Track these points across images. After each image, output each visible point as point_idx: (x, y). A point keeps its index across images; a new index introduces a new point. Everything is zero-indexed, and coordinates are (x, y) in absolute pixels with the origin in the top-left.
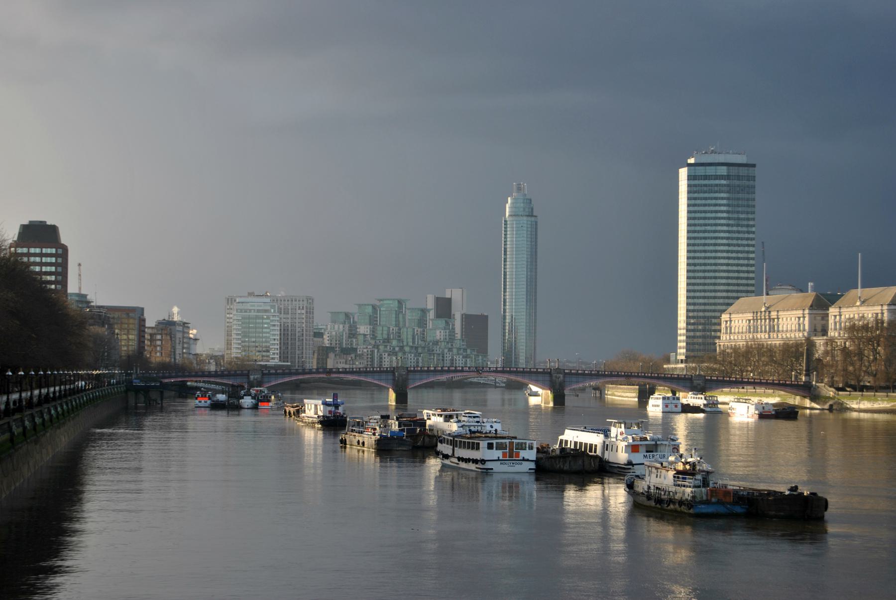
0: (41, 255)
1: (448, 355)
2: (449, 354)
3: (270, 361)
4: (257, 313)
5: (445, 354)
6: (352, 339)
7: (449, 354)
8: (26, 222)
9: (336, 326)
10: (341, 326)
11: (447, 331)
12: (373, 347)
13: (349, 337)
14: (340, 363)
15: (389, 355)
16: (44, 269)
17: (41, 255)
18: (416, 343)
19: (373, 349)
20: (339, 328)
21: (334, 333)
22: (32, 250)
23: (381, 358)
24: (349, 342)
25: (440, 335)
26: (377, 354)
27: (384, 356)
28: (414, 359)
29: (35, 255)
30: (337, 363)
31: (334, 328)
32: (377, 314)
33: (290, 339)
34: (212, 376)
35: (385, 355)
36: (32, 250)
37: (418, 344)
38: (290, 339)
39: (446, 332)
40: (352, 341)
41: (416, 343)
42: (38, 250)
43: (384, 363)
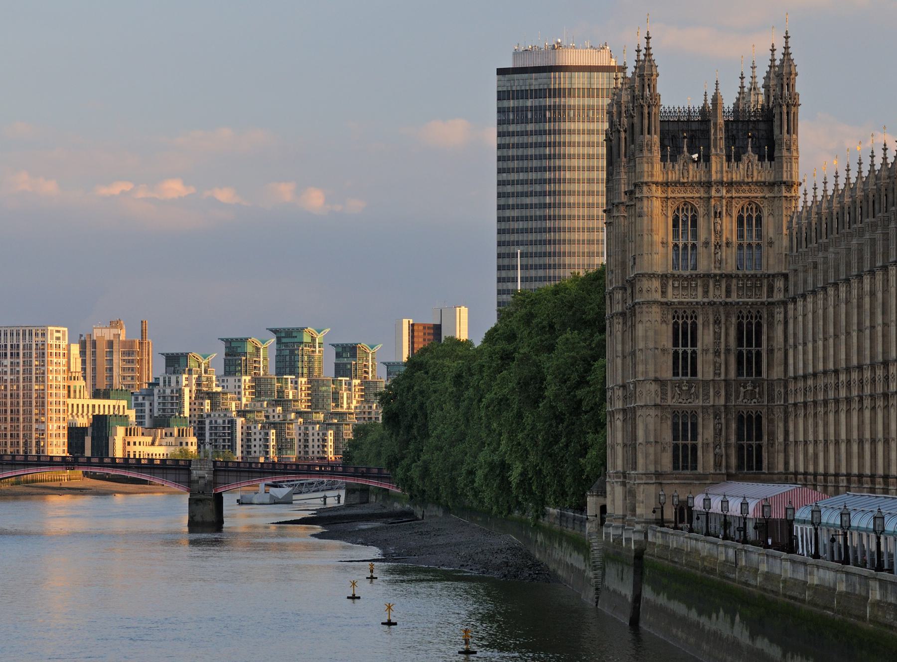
9: (173, 378)
14: (135, 443)
18: (345, 406)
21: (168, 391)
23: (249, 434)
24: (195, 407)
30: (129, 444)
31: (170, 382)
37: (349, 408)
41: (345, 406)
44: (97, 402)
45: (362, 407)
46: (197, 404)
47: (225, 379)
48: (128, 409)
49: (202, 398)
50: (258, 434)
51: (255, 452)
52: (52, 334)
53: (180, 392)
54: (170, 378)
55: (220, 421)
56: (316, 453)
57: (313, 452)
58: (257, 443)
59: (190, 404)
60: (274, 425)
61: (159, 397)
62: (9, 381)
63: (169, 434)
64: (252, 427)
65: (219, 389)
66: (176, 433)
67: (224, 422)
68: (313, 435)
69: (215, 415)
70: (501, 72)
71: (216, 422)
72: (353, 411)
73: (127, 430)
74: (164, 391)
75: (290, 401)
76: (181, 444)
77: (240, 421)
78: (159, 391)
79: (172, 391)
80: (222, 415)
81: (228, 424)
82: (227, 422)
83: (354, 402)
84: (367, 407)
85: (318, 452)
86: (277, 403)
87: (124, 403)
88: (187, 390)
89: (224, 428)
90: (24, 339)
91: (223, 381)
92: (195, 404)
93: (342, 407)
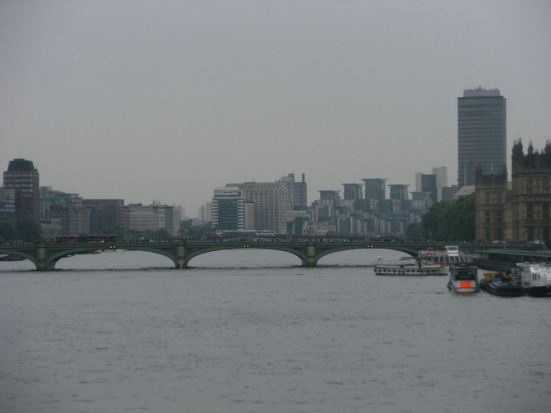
0: (21, 178)
4: (228, 197)
6: (335, 210)
8: (12, 160)
9: (324, 201)
11: (424, 201)
12: (350, 216)
13: (334, 209)
15: (362, 221)
16: (22, 185)
17: (21, 178)
18: (395, 211)
19: (350, 217)
20: (326, 202)
21: (322, 206)
22: (16, 175)
23: (356, 224)
24: (333, 213)
25: (418, 205)
26: (353, 221)
27: (358, 222)
28: (384, 224)
29: (18, 178)
31: (322, 203)
33: (269, 213)
35: (358, 221)
36: (16, 175)
37: (397, 211)
38: (269, 213)
39: (423, 202)
40: (335, 212)
41: (395, 211)
42: (19, 175)
43: (358, 230)
44: (296, 212)
51: (358, 231)
52: (281, 185)
53: (327, 207)
59: (331, 211)
60: (366, 220)
61: (318, 209)
63: (324, 224)
64: (357, 221)
65: (343, 206)
66: (327, 224)
67: (345, 219)
68: (382, 224)
70: (459, 99)
72: (398, 213)
73: (309, 223)
74: (320, 206)
75: (372, 210)
76: (330, 228)
77: (352, 219)
79: (324, 207)
80: (344, 216)
85: (385, 231)
88: (330, 206)
89: (346, 221)
91: (344, 202)
93: (393, 212)
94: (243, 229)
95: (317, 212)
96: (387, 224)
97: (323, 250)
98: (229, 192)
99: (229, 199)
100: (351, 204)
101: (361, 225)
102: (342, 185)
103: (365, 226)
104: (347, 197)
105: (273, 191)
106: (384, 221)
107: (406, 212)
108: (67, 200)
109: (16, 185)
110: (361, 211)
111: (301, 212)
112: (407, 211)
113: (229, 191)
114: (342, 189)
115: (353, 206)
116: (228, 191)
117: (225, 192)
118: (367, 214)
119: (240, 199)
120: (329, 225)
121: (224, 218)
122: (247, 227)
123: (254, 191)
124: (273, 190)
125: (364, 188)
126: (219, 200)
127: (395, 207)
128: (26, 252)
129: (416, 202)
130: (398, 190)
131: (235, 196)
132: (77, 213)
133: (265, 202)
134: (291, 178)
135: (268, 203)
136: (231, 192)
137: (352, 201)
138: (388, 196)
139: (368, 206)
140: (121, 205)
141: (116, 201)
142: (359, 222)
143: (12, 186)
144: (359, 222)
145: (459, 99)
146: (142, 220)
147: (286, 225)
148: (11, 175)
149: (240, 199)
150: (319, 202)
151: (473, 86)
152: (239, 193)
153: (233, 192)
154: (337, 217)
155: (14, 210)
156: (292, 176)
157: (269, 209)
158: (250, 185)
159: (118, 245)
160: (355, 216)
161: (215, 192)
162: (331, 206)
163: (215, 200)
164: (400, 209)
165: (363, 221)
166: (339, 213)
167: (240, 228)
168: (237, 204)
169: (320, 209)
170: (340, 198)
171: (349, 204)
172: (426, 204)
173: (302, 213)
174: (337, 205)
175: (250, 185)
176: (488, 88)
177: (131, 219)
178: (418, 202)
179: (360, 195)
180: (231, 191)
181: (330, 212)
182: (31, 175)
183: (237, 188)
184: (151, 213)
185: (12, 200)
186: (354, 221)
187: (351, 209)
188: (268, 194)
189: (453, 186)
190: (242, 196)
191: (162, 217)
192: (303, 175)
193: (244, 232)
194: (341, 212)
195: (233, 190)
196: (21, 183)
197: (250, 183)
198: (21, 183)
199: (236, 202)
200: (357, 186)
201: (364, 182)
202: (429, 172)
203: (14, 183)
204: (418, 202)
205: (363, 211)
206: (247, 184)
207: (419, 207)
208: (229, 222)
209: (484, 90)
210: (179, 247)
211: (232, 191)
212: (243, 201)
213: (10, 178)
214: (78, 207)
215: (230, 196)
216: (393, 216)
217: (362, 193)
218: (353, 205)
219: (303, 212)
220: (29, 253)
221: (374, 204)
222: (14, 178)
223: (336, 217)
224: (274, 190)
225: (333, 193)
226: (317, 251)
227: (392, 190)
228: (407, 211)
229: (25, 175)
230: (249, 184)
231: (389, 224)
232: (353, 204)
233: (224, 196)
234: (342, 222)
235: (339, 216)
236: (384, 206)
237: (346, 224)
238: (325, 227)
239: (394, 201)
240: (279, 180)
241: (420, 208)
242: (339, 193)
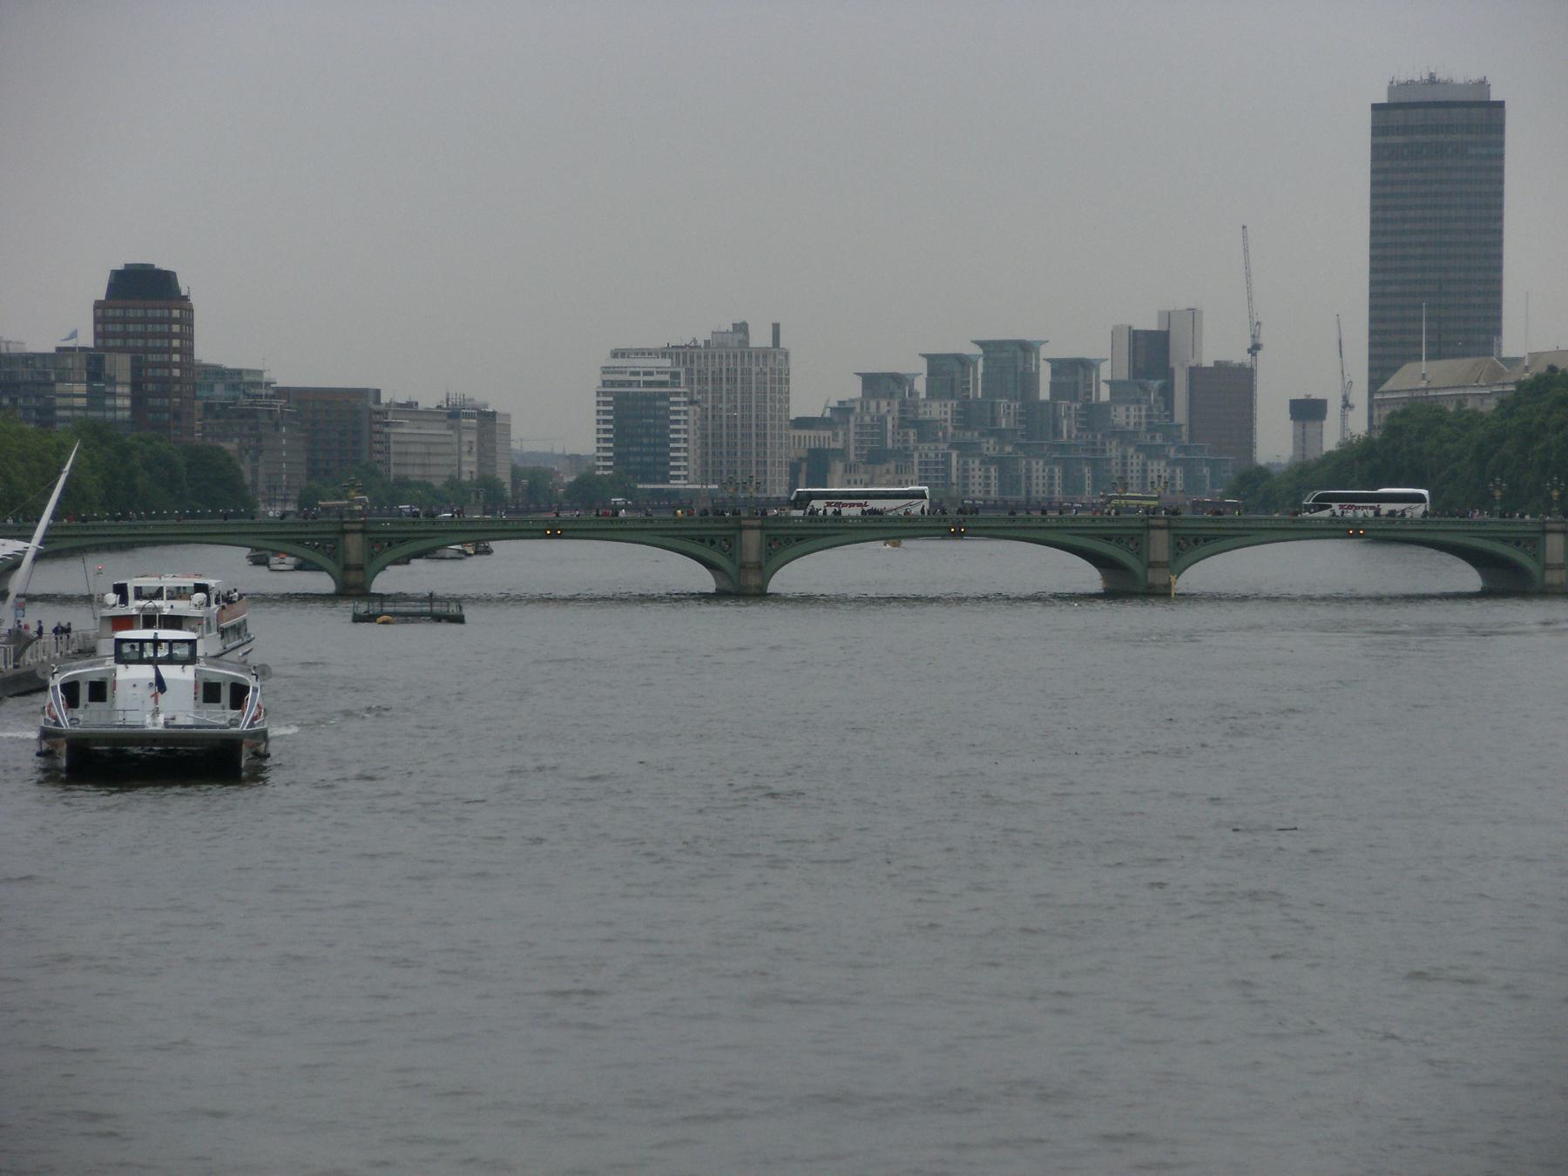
1: (1135, 460)
2: (1138, 457)
3: (671, 482)
5: (1129, 457)
7: (1138, 457)
8: (120, 267)
9: (873, 404)
10: (884, 404)
11: (1144, 407)
13: (900, 426)
15: (982, 463)
16: (150, 343)
17: (144, 321)
19: (950, 451)
20: (878, 407)
21: (867, 419)
22: (131, 313)
23: (966, 470)
24: (900, 437)
25: (1128, 417)
26: (958, 462)
27: (971, 466)
28: (1044, 471)
29: (136, 321)
31: (868, 408)
32: (968, 376)
33: (739, 436)
34: (543, 511)
36: (131, 313)
37: (1069, 437)
38: (739, 436)
39: (1140, 410)
40: (906, 434)
42: (140, 313)
45: (1084, 436)
46: (901, 434)
47: (928, 403)
48: (833, 440)
49: (906, 427)
50: (977, 470)
51: (973, 492)
52: (775, 357)
53: (882, 419)
54: (868, 403)
55: (932, 455)
56: (1041, 492)
57: (1037, 492)
58: (977, 480)
61: (856, 426)
62: (724, 410)
64: (970, 462)
65: (927, 417)
67: (937, 455)
68: (1037, 470)
69: (923, 448)
70: (1375, 107)
71: (927, 456)
72: (1073, 442)
73: (846, 466)
75: (1004, 430)
78: (856, 418)
79: (872, 420)
80: (933, 448)
81: (942, 457)
82: (940, 456)
83: (1074, 432)
84: (1090, 437)
85: (1044, 492)
86: (992, 433)
87: (829, 433)
88: (889, 419)
89: (937, 463)
90: (742, 361)
91: (925, 406)
92: (899, 434)
93: (1062, 437)
94: (686, 482)
95: (852, 435)
96: (1052, 471)
97: (1196, 541)
98: (646, 374)
99: (645, 393)
100: (946, 413)
101: (980, 473)
102: (920, 358)
103: (993, 479)
104: (931, 394)
105: (750, 374)
106: (1041, 463)
107: (1095, 437)
108: (234, 387)
109: (131, 342)
110: (976, 434)
111: (888, 435)
112: (1099, 436)
113: (634, 370)
114: (922, 367)
115: (952, 420)
116: (641, 370)
117: (632, 374)
118: (992, 441)
119: (677, 394)
120: (897, 473)
121: (631, 449)
122: (692, 477)
123: (695, 372)
124: (750, 369)
125: (981, 363)
126: (619, 398)
127: (1065, 422)
128: (703, 541)
129: (1121, 410)
130: (1073, 371)
131: (662, 384)
132: (277, 426)
133: (728, 402)
134: (741, 336)
135: (736, 406)
136: (651, 374)
137: (949, 405)
138: (1044, 394)
139: (994, 420)
140: (375, 407)
141: (360, 393)
142: (975, 464)
143: (119, 342)
144: (975, 464)
145: (1375, 107)
146: (421, 449)
147: (786, 471)
148: (119, 313)
149: (677, 394)
150: (858, 406)
151: (1413, 69)
152: (675, 375)
153: (658, 373)
154: (912, 448)
155: (127, 414)
156: (742, 328)
157: (739, 425)
158: (685, 354)
159: (1369, 527)
160: (964, 448)
161: (604, 373)
162: (893, 418)
163: (605, 394)
164: (1078, 429)
165: (987, 461)
166: (916, 438)
167: (677, 477)
168: (667, 408)
169: (861, 426)
170: (918, 394)
171: (941, 413)
172: (1148, 416)
173: (824, 437)
174: (910, 416)
175: (685, 354)
176: (1459, 79)
177: (393, 448)
178: (1128, 410)
179: (971, 386)
180: (650, 370)
181: (889, 434)
182: (176, 313)
183: (667, 363)
184: (438, 430)
185: (123, 384)
186: (961, 462)
187: (946, 427)
188: (736, 379)
189: (1216, 363)
190: (682, 385)
191: (471, 442)
192: (776, 327)
193: (686, 489)
194: (921, 438)
195: (657, 368)
196: (144, 336)
197: (681, 347)
198: (144, 336)
199: (665, 404)
200: (962, 361)
201: (979, 351)
202: (1152, 324)
203: (126, 335)
204: (1128, 410)
205: (982, 435)
206: (674, 351)
207: (1128, 424)
208: (646, 459)
209: (1447, 84)
210: (1152, 532)
211: (655, 370)
212: (686, 399)
213: (114, 321)
214: (278, 409)
215: (648, 384)
216: (1063, 448)
217: (976, 380)
218: (952, 415)
219: (822, 433)
220: (712, 542)
221: (1007, 413)
222: (125, 321)
223: (906, 449)
224: (754, 369)
225: (898, 379)
226: (1178, 544)
227: (1054, 372)
228: (1099, 436)
229: (158, 313)
230: (680, 350)
231: (1057, 471)
232: (952, 411)
233: (630, 384)
234: (927, 463)
235: (916, 448)
236: (1037, 420)
237: (937, 470)
238: (889, 477)
239: (1063, 404)
240: (1137, 337)
241: (1131, 428)
242: (916, 379)
